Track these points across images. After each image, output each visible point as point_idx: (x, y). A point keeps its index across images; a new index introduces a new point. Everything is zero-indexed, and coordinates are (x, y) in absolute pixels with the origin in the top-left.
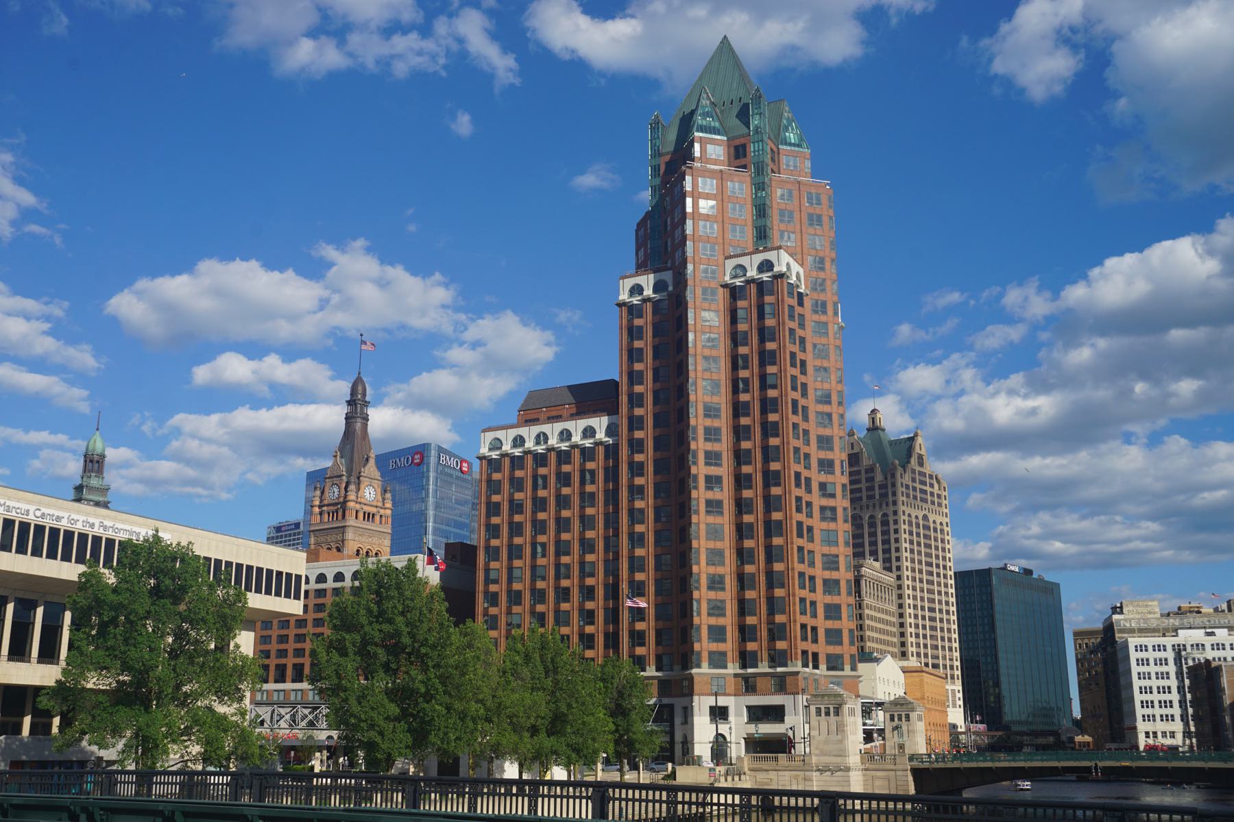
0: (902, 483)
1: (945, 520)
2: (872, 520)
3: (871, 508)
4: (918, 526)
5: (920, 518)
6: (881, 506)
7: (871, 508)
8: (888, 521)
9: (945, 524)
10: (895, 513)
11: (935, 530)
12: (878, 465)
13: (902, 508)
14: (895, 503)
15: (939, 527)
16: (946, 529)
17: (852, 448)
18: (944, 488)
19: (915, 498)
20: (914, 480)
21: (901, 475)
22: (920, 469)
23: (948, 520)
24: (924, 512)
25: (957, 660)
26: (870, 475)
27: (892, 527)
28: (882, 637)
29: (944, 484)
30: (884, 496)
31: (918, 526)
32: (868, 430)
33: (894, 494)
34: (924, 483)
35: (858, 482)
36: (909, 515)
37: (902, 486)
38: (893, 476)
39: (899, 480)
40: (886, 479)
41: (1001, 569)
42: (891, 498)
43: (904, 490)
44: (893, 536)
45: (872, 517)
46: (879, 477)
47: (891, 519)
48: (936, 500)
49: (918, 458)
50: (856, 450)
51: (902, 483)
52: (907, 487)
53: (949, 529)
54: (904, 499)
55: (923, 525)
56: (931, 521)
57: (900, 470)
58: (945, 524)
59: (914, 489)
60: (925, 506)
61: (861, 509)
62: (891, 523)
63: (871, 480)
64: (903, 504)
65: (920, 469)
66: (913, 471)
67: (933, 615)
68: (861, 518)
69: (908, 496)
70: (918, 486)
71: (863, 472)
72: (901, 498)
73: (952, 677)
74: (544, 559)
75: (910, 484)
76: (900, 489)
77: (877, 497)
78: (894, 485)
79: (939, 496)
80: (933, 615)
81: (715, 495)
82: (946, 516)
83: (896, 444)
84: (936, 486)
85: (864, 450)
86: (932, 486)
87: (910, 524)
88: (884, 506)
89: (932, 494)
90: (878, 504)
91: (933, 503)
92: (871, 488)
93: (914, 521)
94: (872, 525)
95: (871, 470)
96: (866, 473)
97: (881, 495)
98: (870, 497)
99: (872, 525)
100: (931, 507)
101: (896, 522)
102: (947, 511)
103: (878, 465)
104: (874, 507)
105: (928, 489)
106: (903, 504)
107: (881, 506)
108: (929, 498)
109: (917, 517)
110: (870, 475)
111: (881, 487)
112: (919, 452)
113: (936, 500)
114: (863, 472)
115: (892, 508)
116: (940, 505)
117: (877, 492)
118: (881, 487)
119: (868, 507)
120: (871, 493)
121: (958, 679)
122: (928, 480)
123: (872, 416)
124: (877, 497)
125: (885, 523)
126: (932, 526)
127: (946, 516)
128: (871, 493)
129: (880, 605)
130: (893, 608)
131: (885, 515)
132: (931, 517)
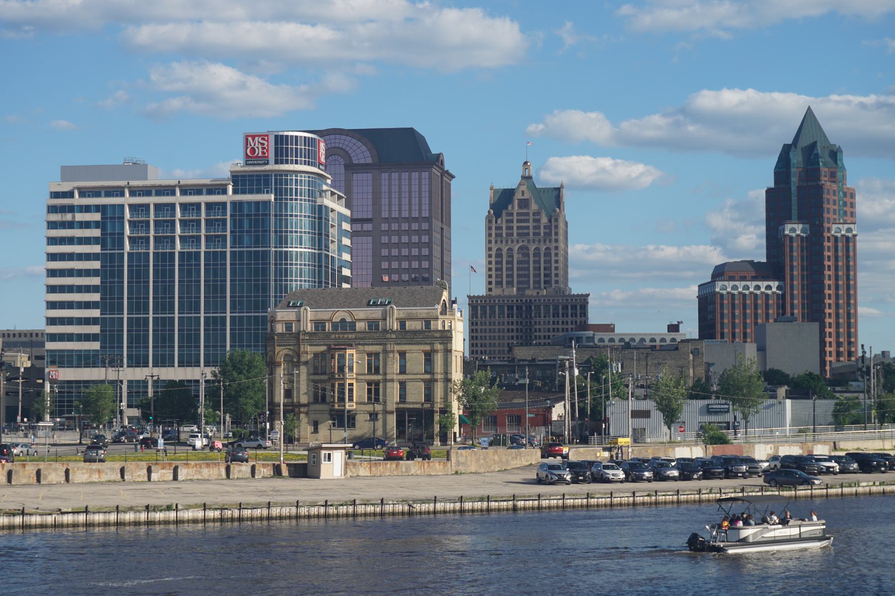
6: (545, 241)
8: (550, 253)
10: (556, 248)
17: (523, 194)
35: (527, 221)
40: (550, 221)
42: (553, 237)
46: (544, 220)
47: (553, 252)
61: (529, 241)
63: (539, 221)
71: (531, 214)
77: (542, 234)
83: (544, 191)
88: (548, 242)
90: (542, 240)
97: (545, 233)
107: (545, 241)
110: (537, 217)
114: (531, 214)
115: (554, 244)
118: (545, 227)
119: (534, 241)
124: (542, 234)
125: (548, 254)
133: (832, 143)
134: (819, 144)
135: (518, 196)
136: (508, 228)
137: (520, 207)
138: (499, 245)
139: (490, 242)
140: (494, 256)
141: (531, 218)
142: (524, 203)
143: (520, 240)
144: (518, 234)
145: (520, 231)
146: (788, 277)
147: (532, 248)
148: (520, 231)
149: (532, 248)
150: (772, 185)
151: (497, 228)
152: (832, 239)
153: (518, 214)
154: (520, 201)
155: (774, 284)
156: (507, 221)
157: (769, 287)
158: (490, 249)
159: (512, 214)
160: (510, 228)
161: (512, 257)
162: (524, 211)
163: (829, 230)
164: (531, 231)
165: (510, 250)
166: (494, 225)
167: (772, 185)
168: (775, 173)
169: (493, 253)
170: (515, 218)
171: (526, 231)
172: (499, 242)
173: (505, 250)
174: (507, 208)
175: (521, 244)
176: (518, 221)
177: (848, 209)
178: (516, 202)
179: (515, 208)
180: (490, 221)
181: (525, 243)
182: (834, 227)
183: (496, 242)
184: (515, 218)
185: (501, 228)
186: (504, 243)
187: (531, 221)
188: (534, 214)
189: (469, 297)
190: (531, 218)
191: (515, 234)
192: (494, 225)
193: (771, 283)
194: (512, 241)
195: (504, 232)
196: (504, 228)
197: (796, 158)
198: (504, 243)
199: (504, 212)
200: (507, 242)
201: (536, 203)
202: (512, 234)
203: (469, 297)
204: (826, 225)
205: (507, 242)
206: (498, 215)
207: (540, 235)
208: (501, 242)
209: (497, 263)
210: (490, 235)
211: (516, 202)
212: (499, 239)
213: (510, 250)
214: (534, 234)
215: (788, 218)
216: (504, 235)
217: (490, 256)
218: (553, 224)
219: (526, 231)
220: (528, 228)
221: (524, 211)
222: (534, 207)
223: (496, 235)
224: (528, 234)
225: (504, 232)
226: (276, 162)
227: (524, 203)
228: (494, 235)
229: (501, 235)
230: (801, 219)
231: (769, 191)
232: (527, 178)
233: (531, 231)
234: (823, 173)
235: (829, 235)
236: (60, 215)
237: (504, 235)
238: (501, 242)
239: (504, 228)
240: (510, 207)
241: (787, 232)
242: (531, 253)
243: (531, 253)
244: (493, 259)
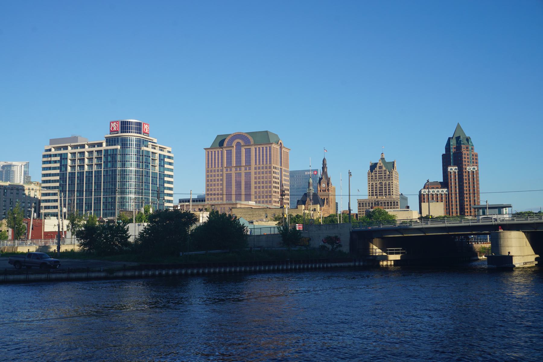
6: (388, 180)
10: (392, 182)
14: (392, 180)
27: (391, 186)
30: (389, 178)
33: (392, 177)
35: (382, 173)
40: (390, 173)
42: (391, 179)
46: (388, 173)
47: (391, 184)
61: (382, 180)
63: (386, 173)
68: (382, 183)
72: (394, 179)
76: (393, 176)
78: (392, 175)
97: (388, 178)
104: (386, 180)
107: (388, 180)
111: (388, 175)
115: (391, 181)
117: (387, 177)
118: (388, 175)
119: (384, 180)
125: (389, 185)
133: (467, 136)
134: (461, 137)
135: (378, 165)
136: (375, 176)
137: (379, 169)
138: (372, 182)
139: (369, 181)
140: (370, 186)
142: (380, 167)
144: (379, 178)
145: (380, 177)
146: (450, 187)
147: (384, 183)
148: (380, 177)
149: (384, 183)
150: (444, 153)
151: (371, 176)
152: (467, 172)
153: (379, 171)
154: (379, 167)
155: (445, 190)
156: (375, 174)
157: (442, 191)
158: (369, 184)
159: (376, 171)
161: (377, 186)
162: (381, 170)
163: (466, 169)
164: (383, 177)
165: (376, 183)
166: (370, 175)
167: (444, 153)
168: (446, 148)
169: (370, 185)
170: (378, 172)
171: (381, 177)
174: (375, 169)
175: (380, 181)
176: (378, 174)
177: (475, 161)
178: (378, 167)
179: (377, 169)
180: (369, 174)
181: (381, 181)
182: (468, 168)
183: (371, 181)
184: (378, 172)
185: (373, 176)
188: (384, 171)
189: (357, 200)
192: (370, 175)
193: (443, 190)
194: (377, 181)
195: (374, 177)
196: (374, 176)
197: (453, 143)
199: (374, 171)
200: (375, 181)
201: (385, 167)
202: (377, 178)
203: (357, 200)
204: (464, 167)
205: (375, 181)
206: (372, 171)
208: (373, 181)
209: (372, 188)
210: (369, 179)
211: (378, 167)
214: (384, 178)
215: (450, 165)
216: (374, 178)
217: (369, 186)
218: (391, 174)
219: (381, 177)
220: (382, 176)
221: (381, 170)
222: (384, 168)
223: (371, 179)
224: (382, 178)
225: (374, 177)
226: (121, 133)
227: (380, 167)
229: (373, 179)
230: (455, 165)
231: (443, 155)
232: (383, 159)
233: (383, 177)
234: (463, 147)
235: (466, 170)
236: (46, 158)
237: (374, 178)
238: (373, 181)
239: (374, 176)
240: (376, 169)
241: (449, 170)
242: (383, 184)
243: (383, 184)
244: (370, 187)
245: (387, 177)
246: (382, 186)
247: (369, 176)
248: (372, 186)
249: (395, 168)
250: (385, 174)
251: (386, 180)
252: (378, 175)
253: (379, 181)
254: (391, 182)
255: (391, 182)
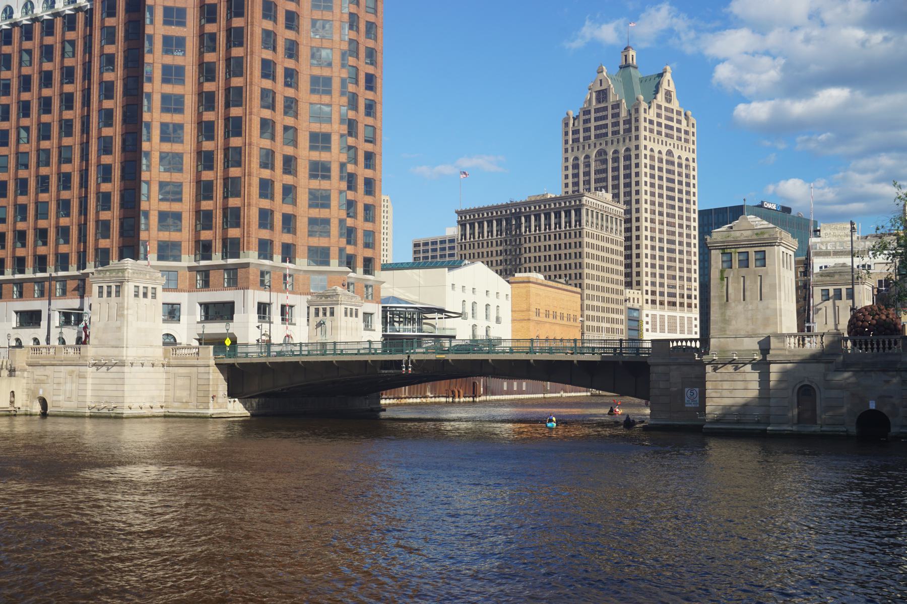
0: (645, 119)
1: (691, 156)
2: (616, 155)
3: (615, 143)
4: (661, 161)
5: (664, 153)
6: (624, 141)
7: (615, 143)
8: (630, 155)
9: (691, 160)
10: (637, 147)
11: (680, 165)
12: (624, 101)
13: (643, 143)
14: (637, 138)
15: (684, 162)
16: (692, 164)
17: (601, 85)
18: (693, 125)
19: (659, 133)
20: (659, 115)
21: (645, 110)
22: (668, 105)
23: (695, 156)
24: (668, 147)
25: (695, 290)
26: (616, 111)
27: (634, 161)
28: (605, 265)
29: (693, 120)
30: (629, 131)
31: (661, 161)
32: (621, 67)
33: (637, 129)
34: (671, 119)
36: (652, 150)
37: (645, 121)
38: (637, 111)
39: (642, 115)
41: (758, 206)
42: (634, 133)
43: (647, 124)
44: (634, 170)
45: (616, 152)
46: (624, 114)
48: (683, 136)
49: (666, 94)
50: (603, 87)
51: (645, 119)
52: (651, 122)
53: (695, 165)
54: (647, 134)
55: (666, 160)
56: (676, 156)
57: (644, 105)
58: (691, 160)
59: (659, 124)
60: (669, 141)
61: (606, 144)
62: (633, 157)
64: (645, 139)
65: (668, 105)
66: (659, 107)
67: (672, 247)
68: (606, 153)
69: (651, 131)
70: (664, 121)
71: (610, 108)
72: (643, 133)
73: (689, 306)
74: (27, 145)
75: (655, 119)
76: (643, 124)
77: (622, 132)
78: (637, 120)
79: (686, 132)
80: (672, 247)
81: (175, 59)
82: (693, 152)
84: (684, 122)
85: (612, 86)
86: (679, 122)
87: (652, 158)
88: (627, 141)
89: (679, 130)
90: (622, 139)
91: (679, 139)
92: (616, 124)
93: (657, 155)
94: (616, 160)
95: (617, 106)
96: (613, 109)
97: (625, 131)
98: (615, 133)
99: (616, 160)
100: (677, 142)
101: (637, 156)
102: (695, 147)
103: (624, 101)
104: (618, 142)
105: (674, 124)
106: (645, 139)
107: (624, 141)
108: (675, 133)
109: (660, 152)
110: (616, 111)
111: (625, 122)
112: (667, 88)
113: (683, 136)
114: (610, 108)
115: (634, 143)
116: (686, 141)
117: (622, 127)
120: (616, 129)
121: (696, 307)
122: (675, 116)
123: (625, 54)
124: (622, 132)
125: (628, 158)
126: (676, 161)
127: (693, 152)
128: (616, 129)
129: (604, 234)
130: (621, 238)
131: (628, 150)
132: (676, 153)
138: (576, 153)
139: (566, 151)
141: (610, 112)
143: (598, 145)
144: (597, 136)
145: (598, 132)
148: (598, 132)
153: (597, 111)
158: (567, 159)
160: (587, 130)
172: (575, 149)
173: (582, 158)
181: (603, 146)
186: (581, 149)
187: (610, 116)
190: (610, 112)
191: (593, 137)
195: (581, 135)
196: (581, 131)
198: (581, 149)
200: (584, 149)
202: (589, 138)
205: (584, 149)
207: (619, 133)
208: (578, 150)
210: (566, 142)
212: (576, 145)
213: (587, 157)
216: (581, 140)
217: (567, 168)
220: (606, 126)
224: (606, 134)
225: (581, 135)
228: (570, 142)
237: (581, 140)
238: (578, 150)
239: (581, 131)
245: (622, 127)
246: (604, 166)
247: (566, 134)
248: (576, 166)
249: (661, 97)
250: (614, 120)
251: (618, 142)
252: (593, 124)
253: (595, 147)
254: (633, 148)
255: (633, 148)
